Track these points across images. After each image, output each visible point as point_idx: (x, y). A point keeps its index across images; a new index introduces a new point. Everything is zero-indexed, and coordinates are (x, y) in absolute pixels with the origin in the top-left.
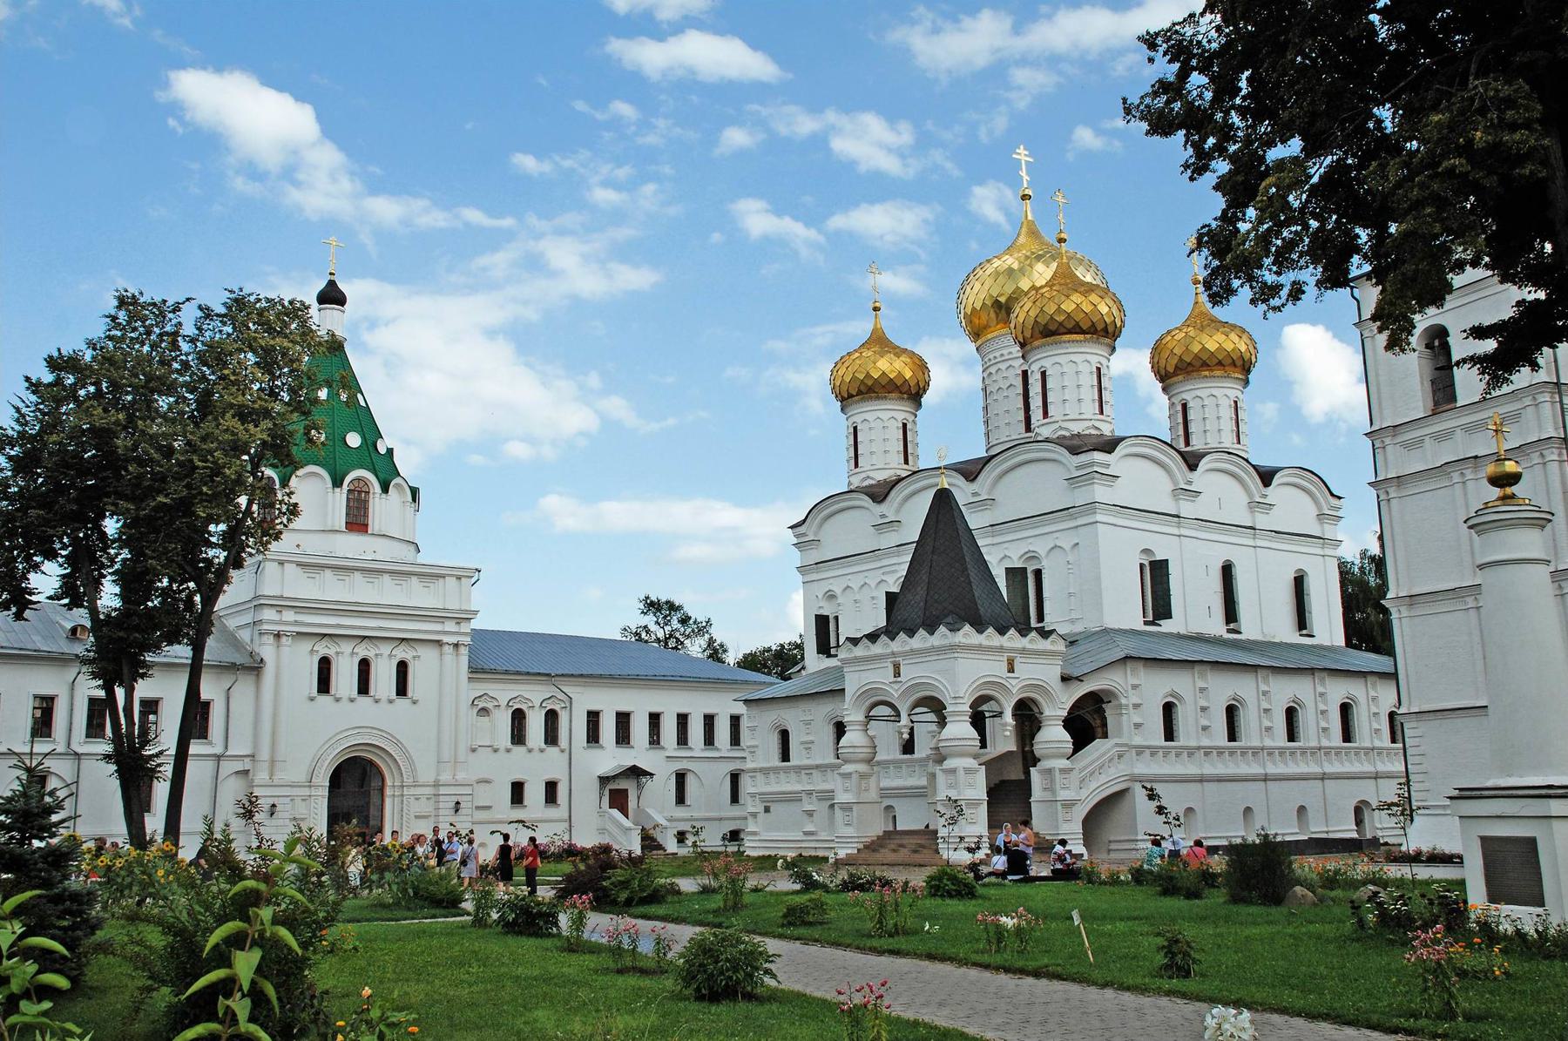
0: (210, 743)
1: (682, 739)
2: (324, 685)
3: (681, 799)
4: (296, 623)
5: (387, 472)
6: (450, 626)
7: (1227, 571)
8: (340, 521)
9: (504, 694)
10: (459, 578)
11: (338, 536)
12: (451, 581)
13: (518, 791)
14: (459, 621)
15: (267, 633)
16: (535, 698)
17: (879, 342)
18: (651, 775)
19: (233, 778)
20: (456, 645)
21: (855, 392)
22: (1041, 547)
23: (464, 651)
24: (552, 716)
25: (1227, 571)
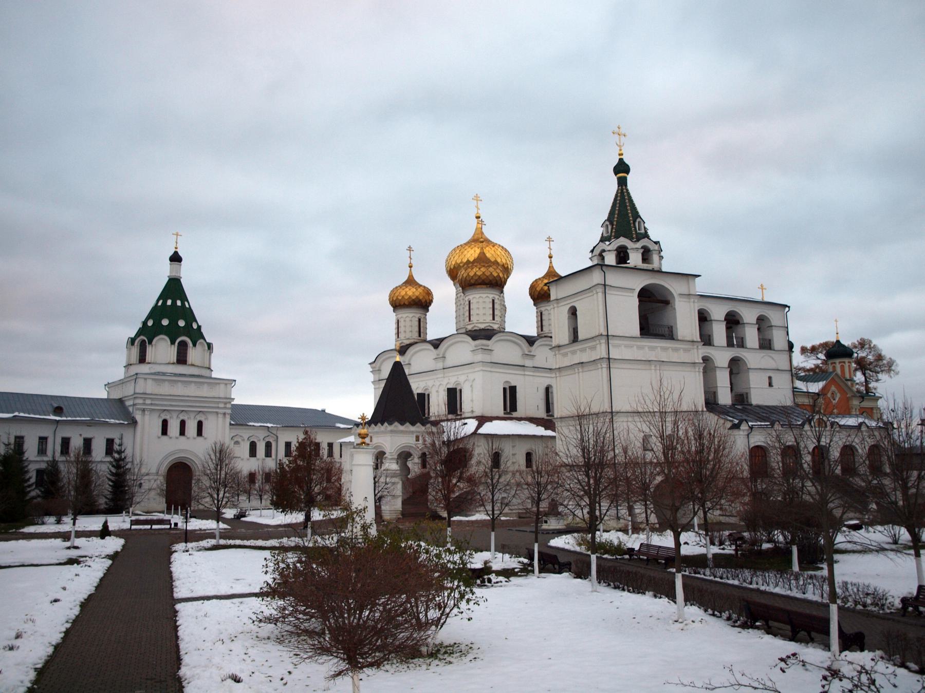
2: (164, 431)
5: (197, 335)
7: (548, 390)
8: (174, 358)
12: (222, 386)
15: (138, 409)
17: (411, 281)
20: (225, 414)
21: (397, 304)
22: (462, 379)
23: (228, 417)
24: (268, 446)
25: (548, 390)
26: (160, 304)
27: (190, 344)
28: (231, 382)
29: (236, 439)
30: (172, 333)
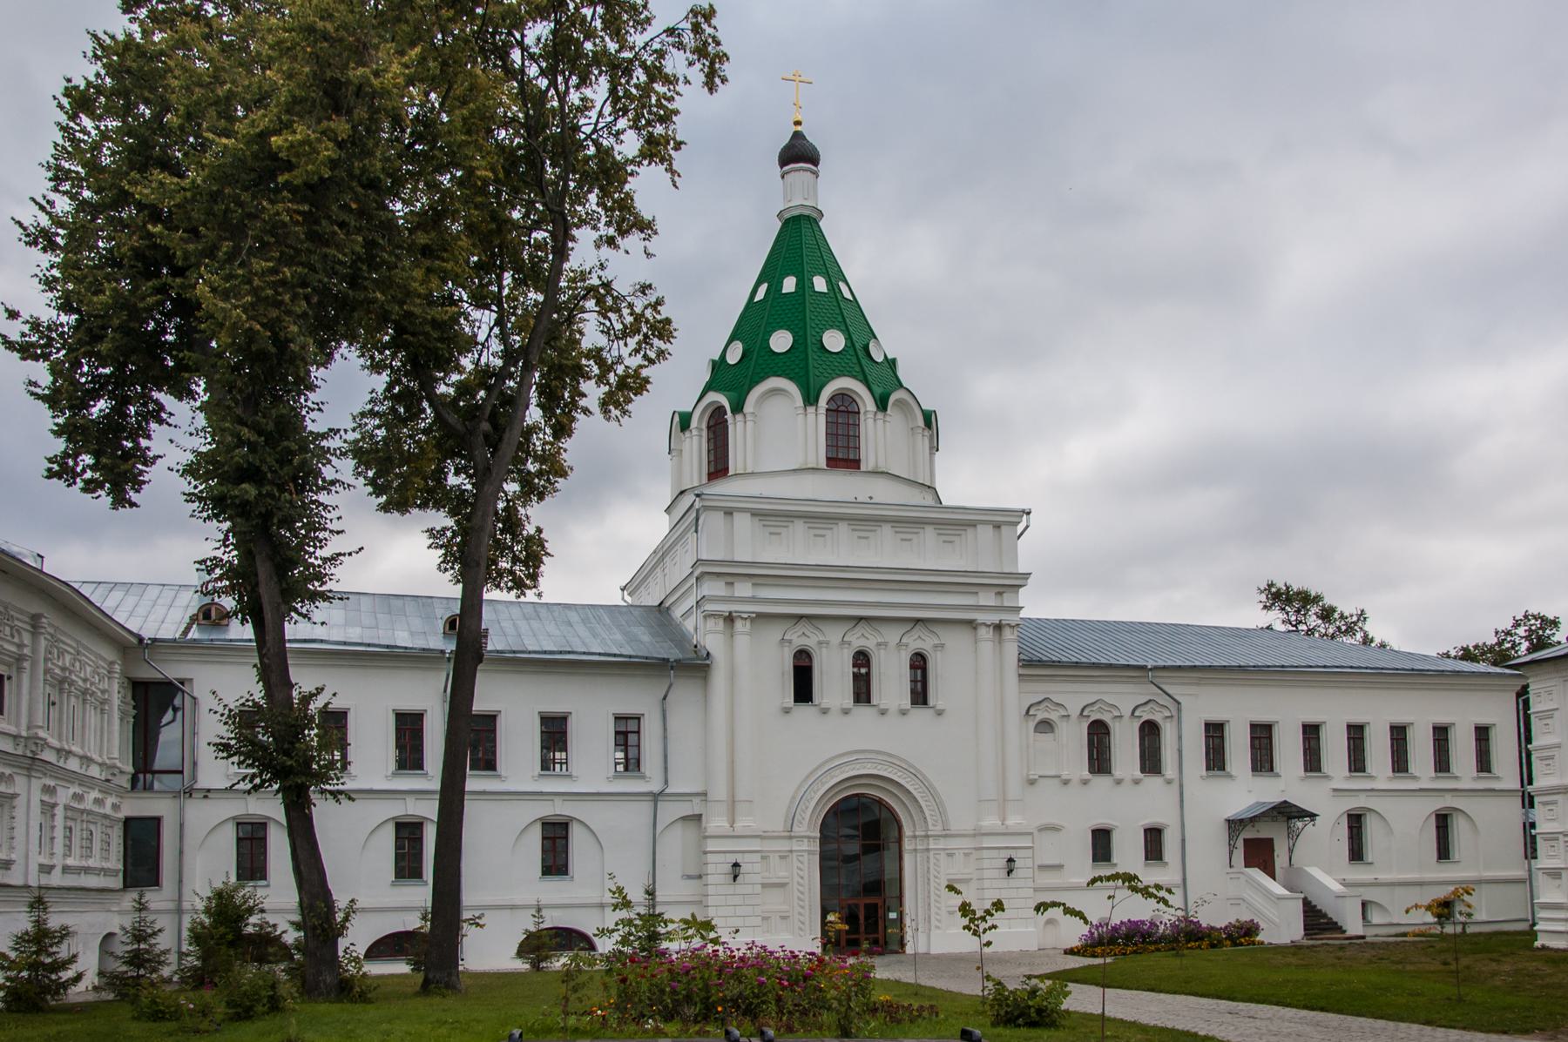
0: (643, 777)
1: (1357, 762)
2: (803, 689)
3: (1357, 853)
4: (753, 600)
5: (885, 382)
6: (987, 599)
9: (1074, 697)
10: (997, 526)
12: (985, 532)
13: (1102, 842)
14: (1001, 590)
16: (1123, 704)
18: (1313, 816)
19: (678, 830)
20: (998, 627)
24: (1150, 731)
26: (760, 296)
27: (867, 403)
28: (1005, 521)
29: (1041, 716)
30: (806, 370)
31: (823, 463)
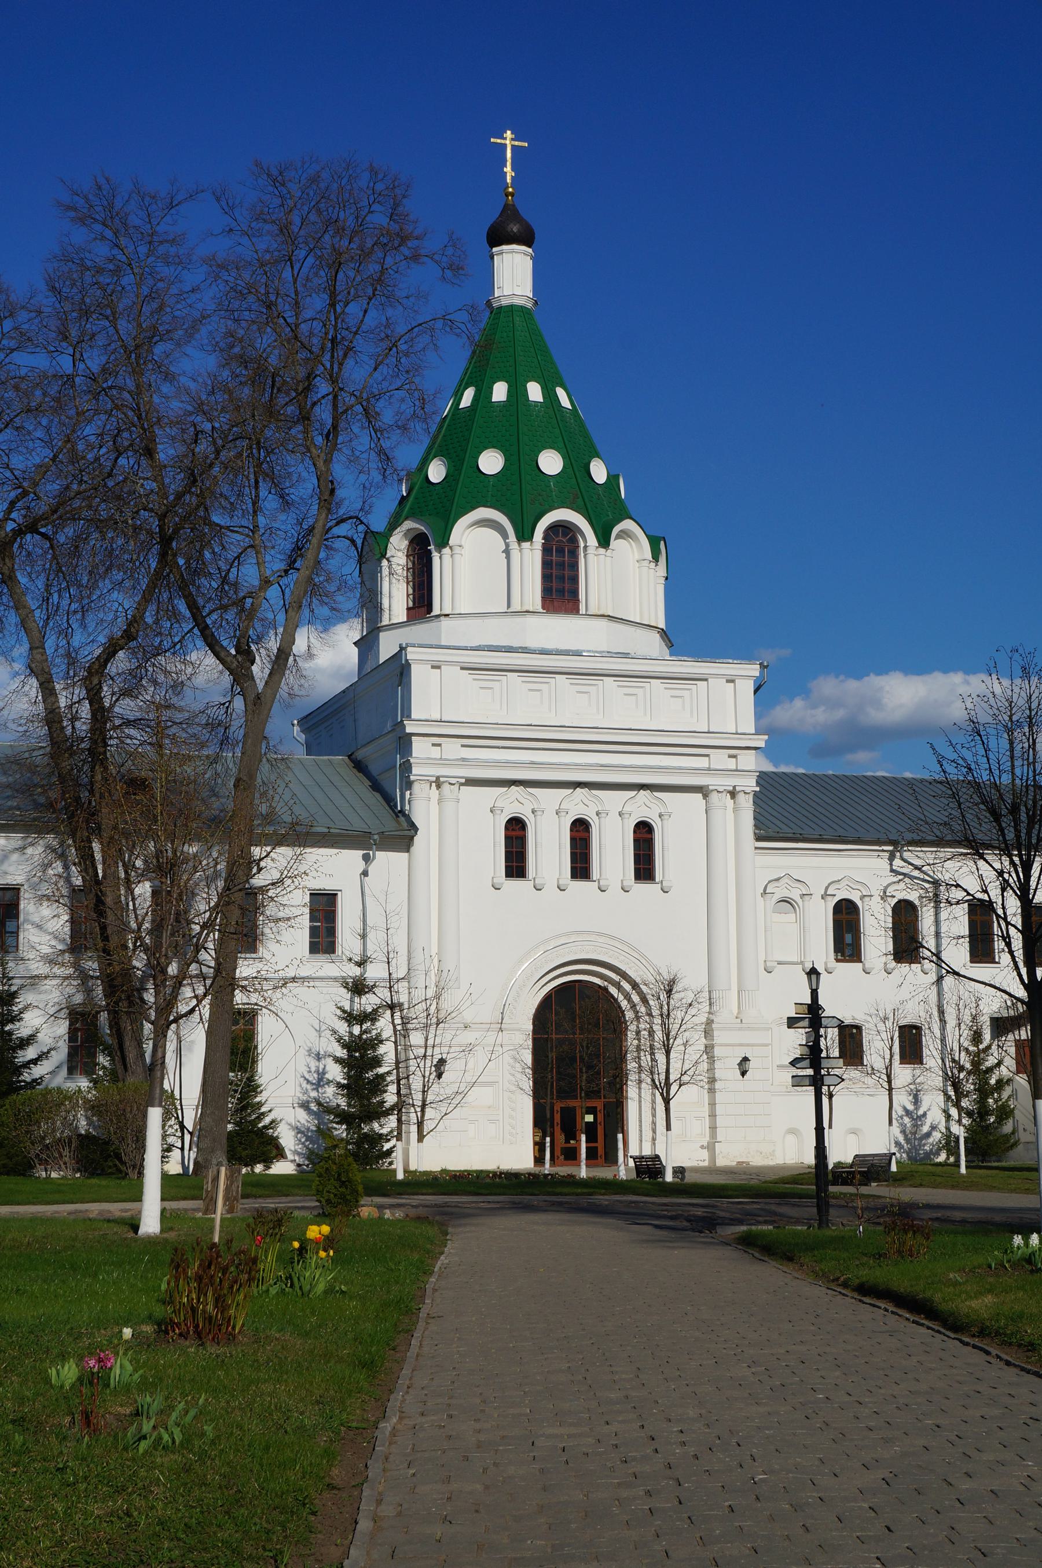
2: (516, 865)
6: (720, 760)
11: (531, 620)
23: (747, 804)
27: (592, 540)
29: (781, 892)
30: (519, 501)
31: (538, 607)
